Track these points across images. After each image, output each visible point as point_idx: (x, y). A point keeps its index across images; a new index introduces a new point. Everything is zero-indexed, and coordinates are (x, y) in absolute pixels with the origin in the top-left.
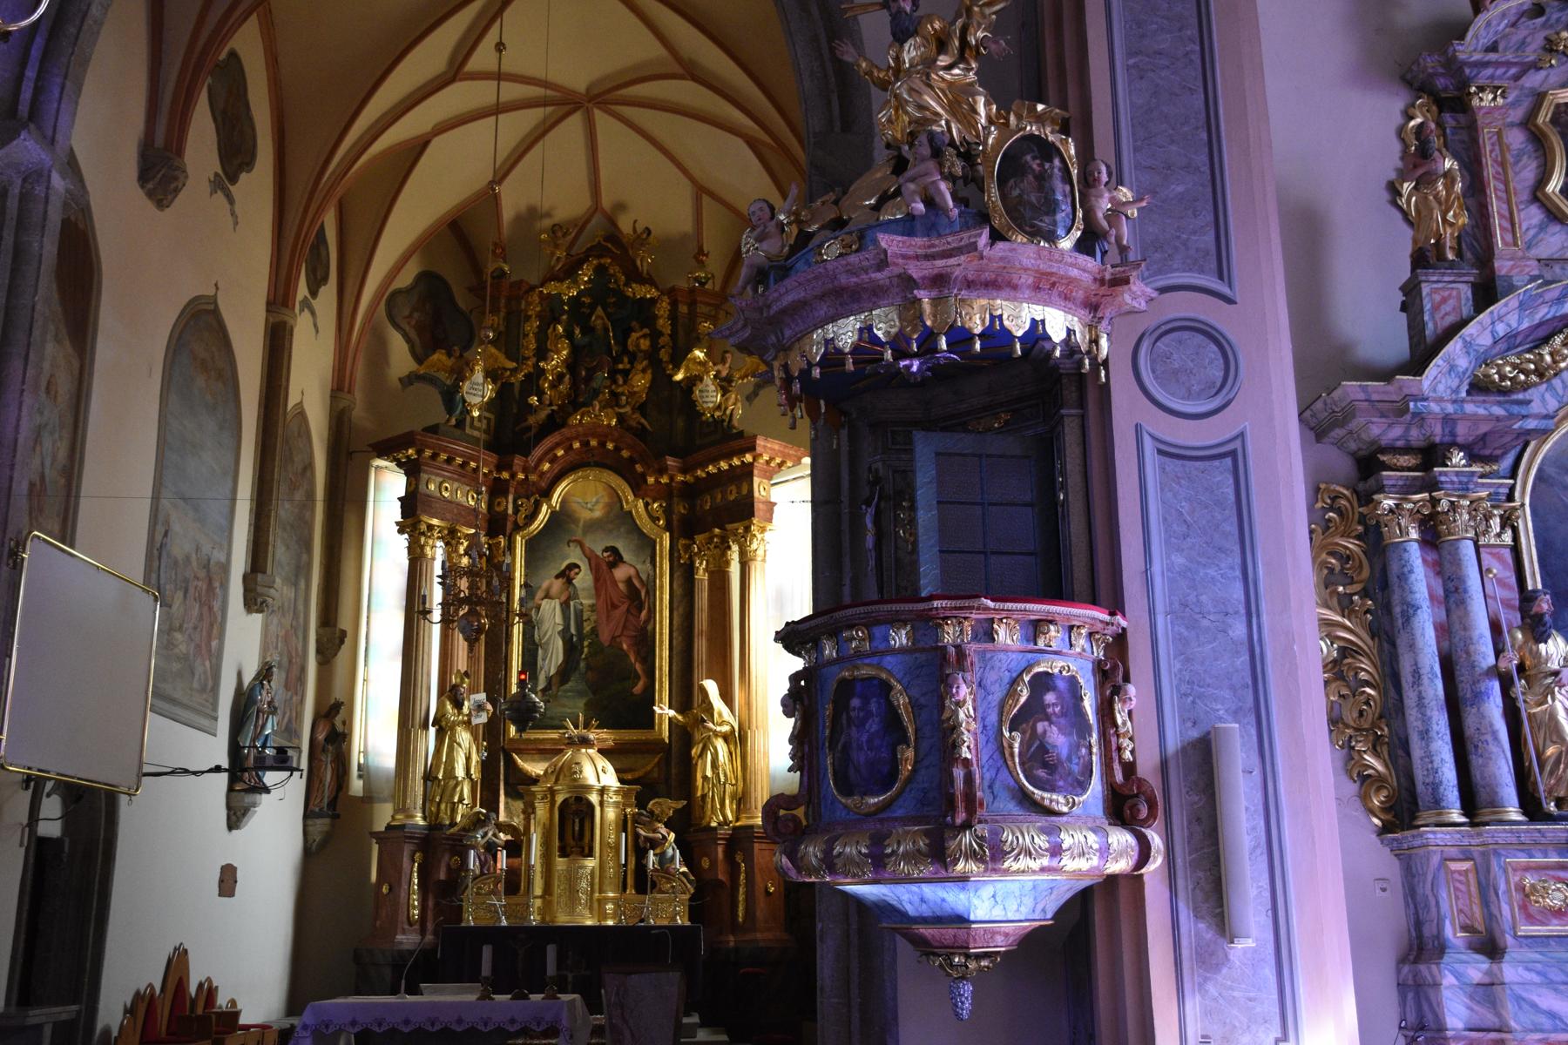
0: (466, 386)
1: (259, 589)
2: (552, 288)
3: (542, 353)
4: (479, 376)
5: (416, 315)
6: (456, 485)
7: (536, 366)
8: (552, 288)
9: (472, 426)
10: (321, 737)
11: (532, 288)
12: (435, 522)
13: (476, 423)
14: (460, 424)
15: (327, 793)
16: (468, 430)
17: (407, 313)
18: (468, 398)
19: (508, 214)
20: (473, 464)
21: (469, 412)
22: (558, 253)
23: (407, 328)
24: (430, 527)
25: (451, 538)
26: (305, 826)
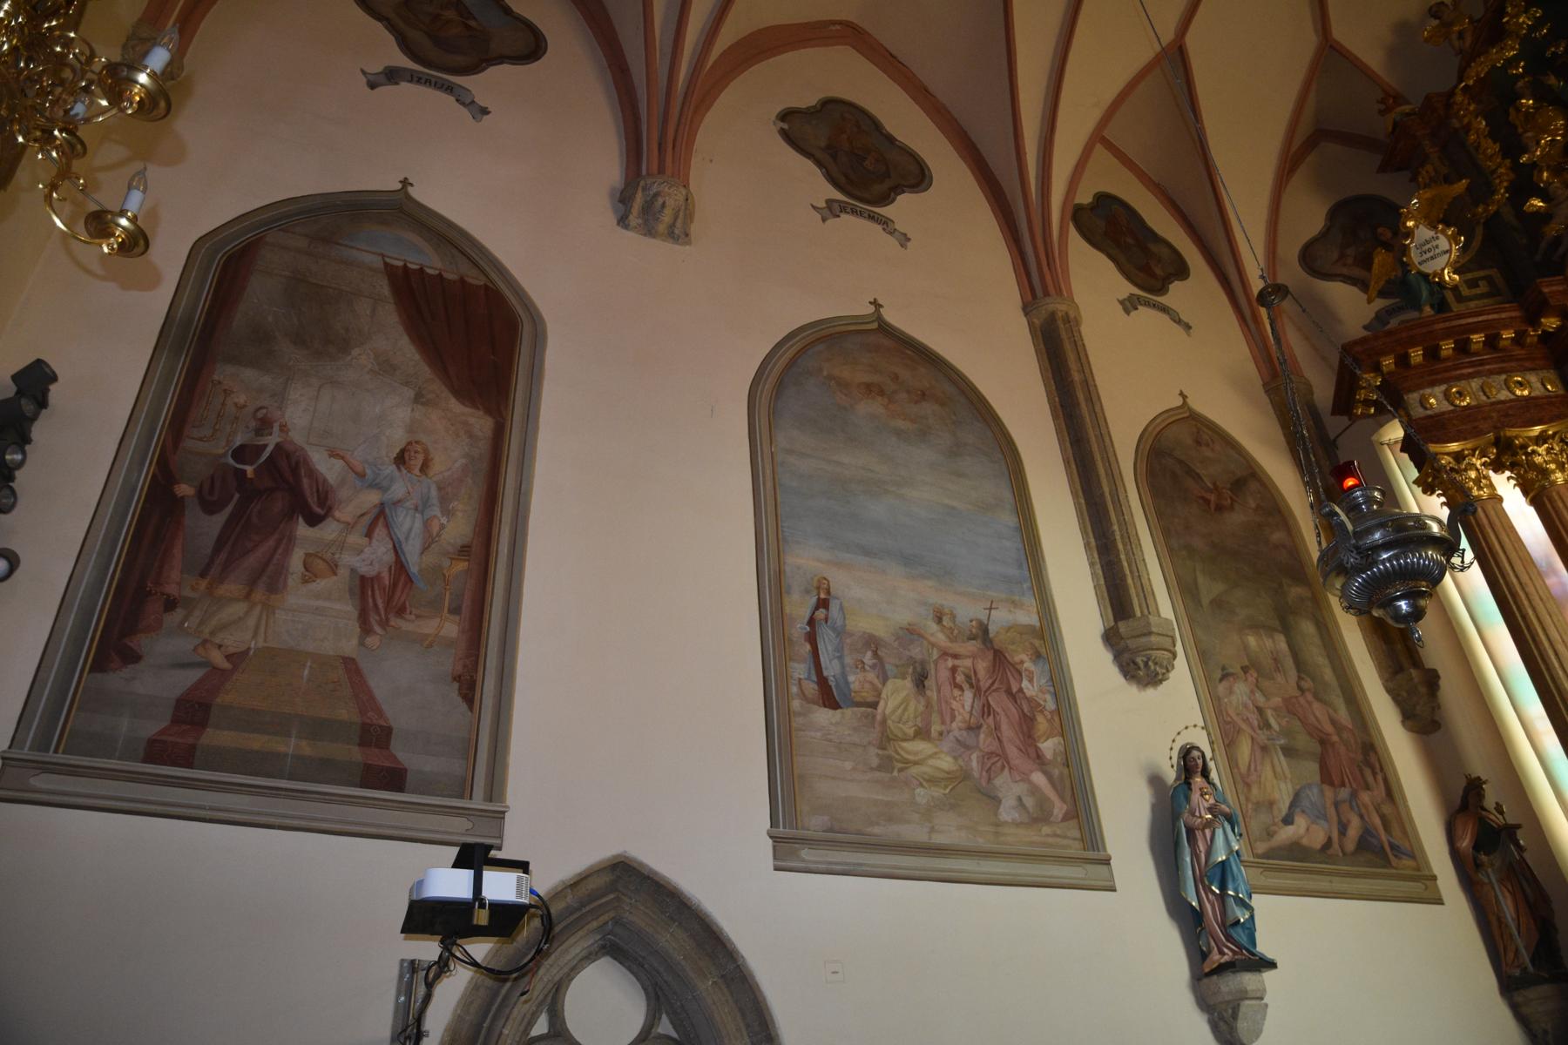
0: (1415, 256)
1: (1132, 644)
2: (1480, 69)
3: (1512, 147)
4: (1424, 233)
5: (1351, 251)
6: (1475, 384)
7: (1516, 167)
8: (1480, 69)
9: (1460, 299)
10: (1465, 843)
11: (1452, 94)
12: (1454, 446)
13: (1465, 291)
14: (1441, 306)
15: (1520, 943)
16: (1456, 308)
17: (1335, 255)
18: (1428, 268)
19: (1373, 58)
20: (1477, 338)
21: (1442, 284)
22: (1456, 28)
23: (1345, 271)
24: (1458, 457)
25: (1507, 456)
26: (1515, 1008)
